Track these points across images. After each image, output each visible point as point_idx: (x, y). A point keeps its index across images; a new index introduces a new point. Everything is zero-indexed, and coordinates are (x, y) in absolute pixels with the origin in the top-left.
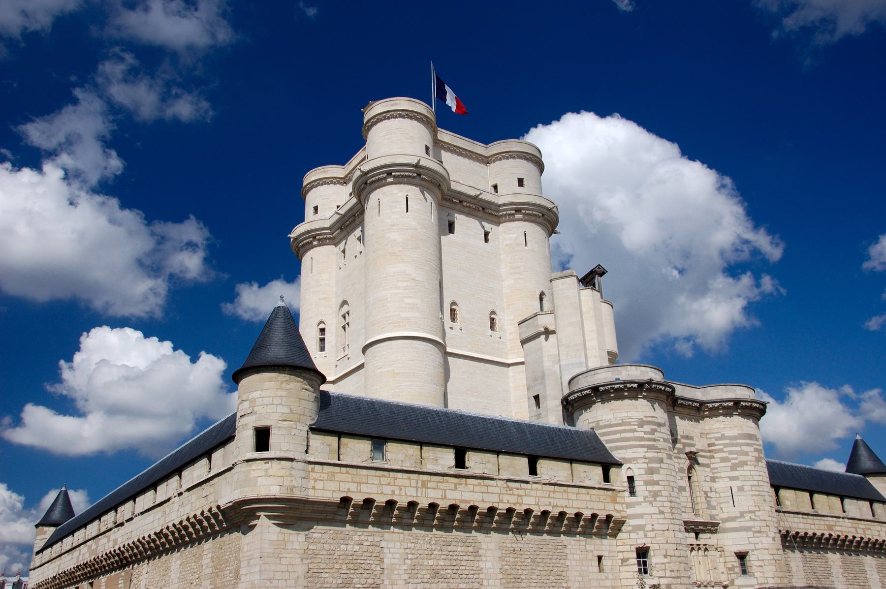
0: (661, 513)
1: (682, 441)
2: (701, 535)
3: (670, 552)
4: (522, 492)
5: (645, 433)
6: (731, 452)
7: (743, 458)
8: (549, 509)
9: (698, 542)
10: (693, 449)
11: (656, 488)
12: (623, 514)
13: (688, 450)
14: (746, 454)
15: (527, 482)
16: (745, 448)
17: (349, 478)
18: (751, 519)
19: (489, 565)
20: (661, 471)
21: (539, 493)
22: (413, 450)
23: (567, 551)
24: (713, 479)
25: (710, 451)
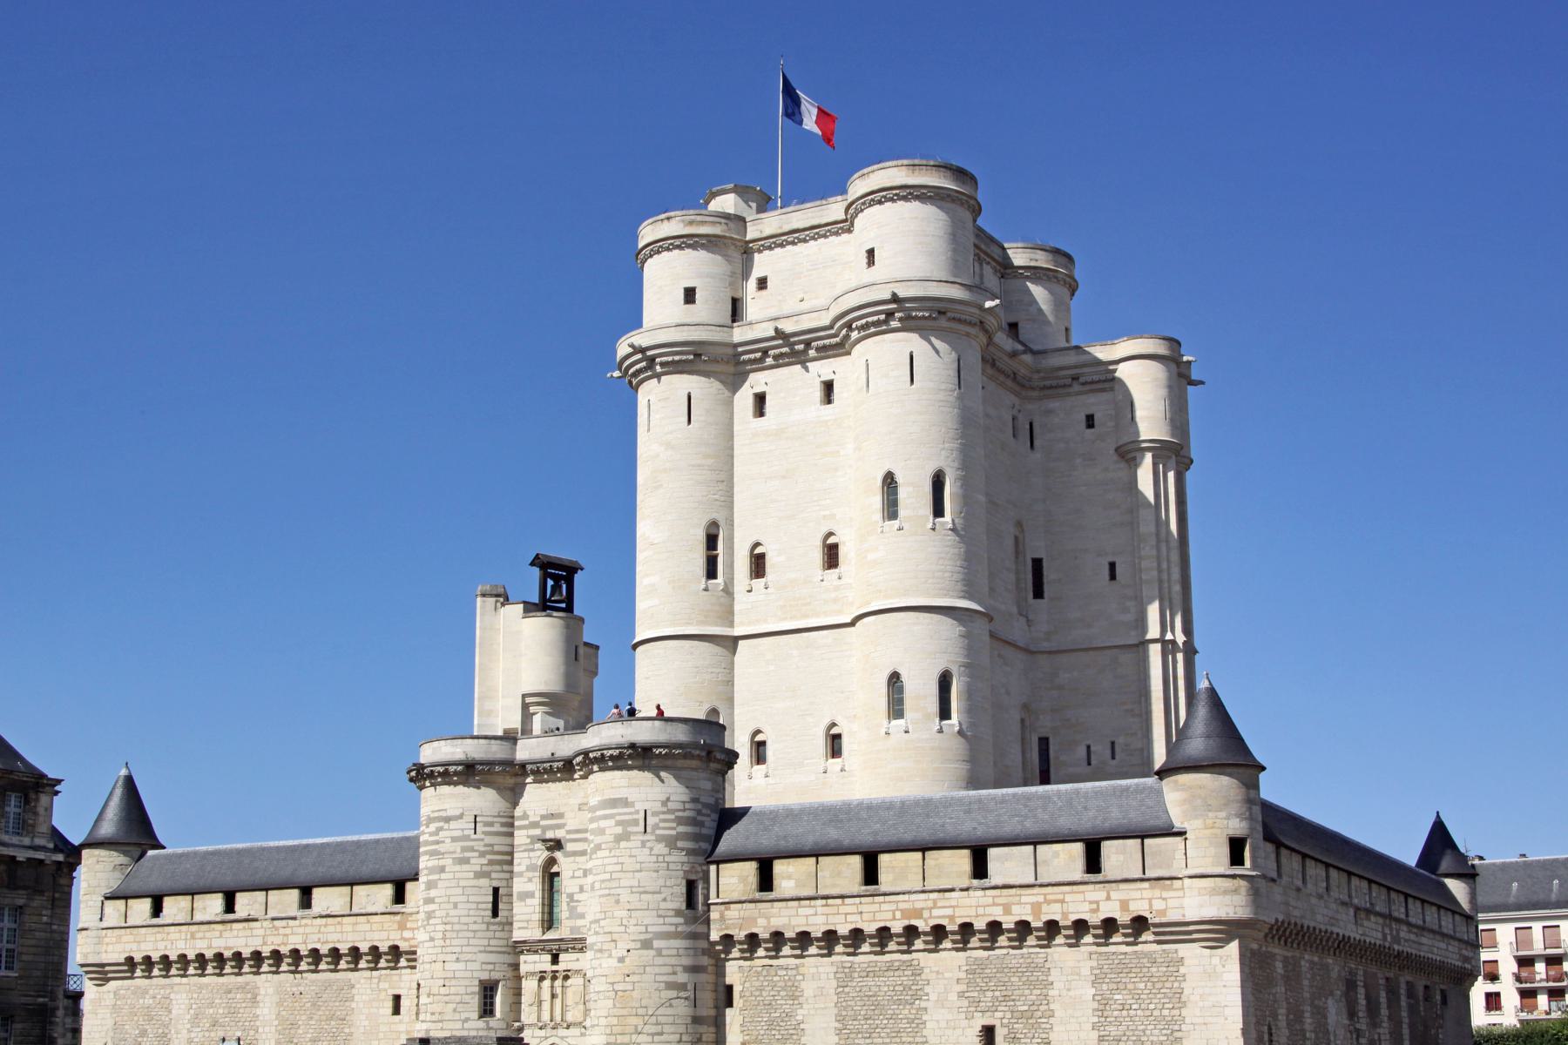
0: (432, 939)
1: (543, 823)
2: (562, 957)
3: (435, 991)
4: (288, 931)
5: (431, 834)
6: (593, 832)
7: (598, 839)
8: (318, 946)
9: (555, 968)
10: (559, 834)
11: (431, 907)
12: (413, 943)
13: (550, 835)
14: (602, 832)
15: (294, 918)
16: (603, 824)
17: (131, 938)
18: (597, 933)
19: (266, 1011)
20: (440, 884)
21: (308, 930)
22: (184, 901)
23: (354, 991)
24: (585, 875)
25: (586, 831)
